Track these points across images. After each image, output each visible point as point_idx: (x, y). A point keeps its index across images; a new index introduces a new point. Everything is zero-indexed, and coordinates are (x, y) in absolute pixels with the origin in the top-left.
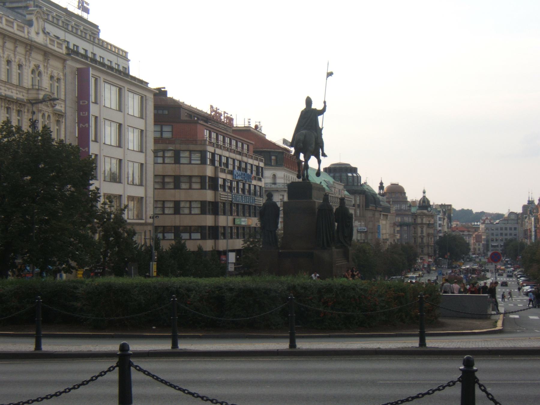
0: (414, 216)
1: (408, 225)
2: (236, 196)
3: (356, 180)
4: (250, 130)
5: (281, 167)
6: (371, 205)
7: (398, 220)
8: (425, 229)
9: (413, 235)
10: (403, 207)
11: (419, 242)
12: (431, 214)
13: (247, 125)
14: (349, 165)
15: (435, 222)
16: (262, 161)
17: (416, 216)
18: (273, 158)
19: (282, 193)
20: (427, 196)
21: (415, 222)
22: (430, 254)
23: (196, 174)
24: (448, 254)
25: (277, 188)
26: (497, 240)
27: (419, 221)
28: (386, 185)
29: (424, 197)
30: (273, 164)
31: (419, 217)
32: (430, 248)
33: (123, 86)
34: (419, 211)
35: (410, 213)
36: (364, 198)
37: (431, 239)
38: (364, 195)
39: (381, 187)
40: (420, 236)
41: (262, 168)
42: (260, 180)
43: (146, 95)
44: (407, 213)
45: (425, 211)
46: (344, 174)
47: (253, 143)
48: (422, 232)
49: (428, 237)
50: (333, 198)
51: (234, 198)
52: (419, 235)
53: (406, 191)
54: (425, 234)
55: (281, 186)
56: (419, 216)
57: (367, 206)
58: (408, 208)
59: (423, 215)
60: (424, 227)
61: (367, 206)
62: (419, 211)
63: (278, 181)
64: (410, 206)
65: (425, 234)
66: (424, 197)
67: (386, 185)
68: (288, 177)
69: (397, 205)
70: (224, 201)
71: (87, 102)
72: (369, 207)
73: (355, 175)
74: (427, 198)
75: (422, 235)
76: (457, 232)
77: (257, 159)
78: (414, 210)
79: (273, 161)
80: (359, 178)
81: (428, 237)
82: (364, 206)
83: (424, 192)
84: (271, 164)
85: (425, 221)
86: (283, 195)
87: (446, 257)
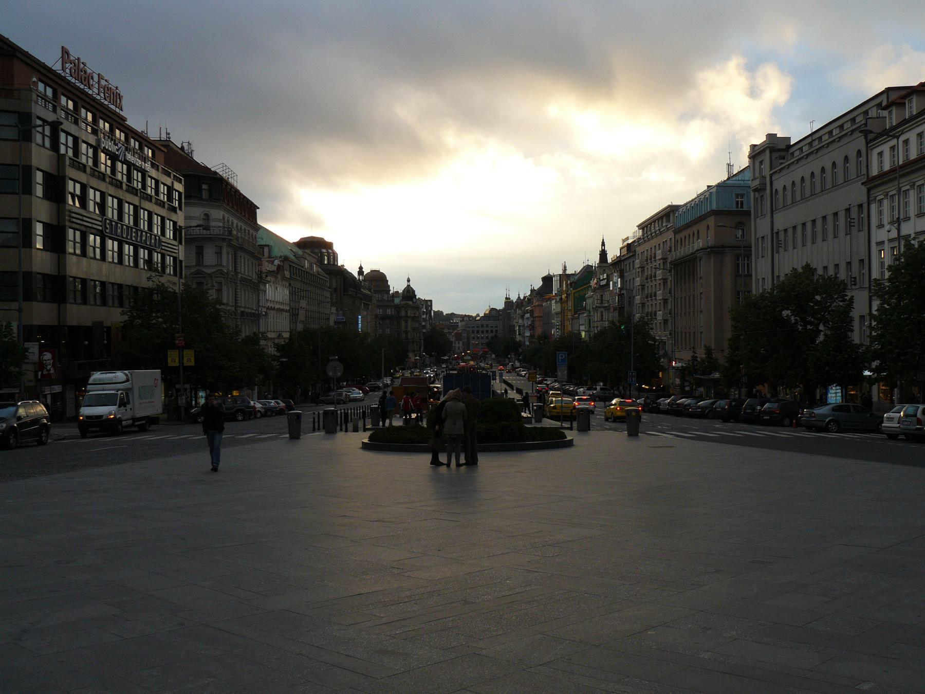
0: (398, 308)
2: (114, 223)
4: (169, 145)
6: (351, 289)
7: (380, 312)
10: (385, 297)
13: (164, 137)
15: (420, 316)
16: (180, 181)
18: (204, 187)
25: (210, 234)
26: (478, 338)
27: (403, 313)
28: (366, 271)
29: (409, 286)
30: (204, 197)
31: (403, 309)
32: (415, 344)
35: (393, 304)
37: (417, 334)
39: (361, 271)
40: (404, 331)
42: (174, 210)
45: (410, 303)
46: (317, 250)
50: (303, 272)
51: (108, 226)
55: (216, 231)
63: (213, 224)
66: (409, 286)
67: (366, 271)
68: (226, 220)
70: (83, 228)
72: (348, 292)
73: (330, 251)
77: (169, 175)
78: (397, 301)
79: (204, 192)
80: (336, 255)
83: (409, 281)
84: (201, 195)
86: (221, 247)
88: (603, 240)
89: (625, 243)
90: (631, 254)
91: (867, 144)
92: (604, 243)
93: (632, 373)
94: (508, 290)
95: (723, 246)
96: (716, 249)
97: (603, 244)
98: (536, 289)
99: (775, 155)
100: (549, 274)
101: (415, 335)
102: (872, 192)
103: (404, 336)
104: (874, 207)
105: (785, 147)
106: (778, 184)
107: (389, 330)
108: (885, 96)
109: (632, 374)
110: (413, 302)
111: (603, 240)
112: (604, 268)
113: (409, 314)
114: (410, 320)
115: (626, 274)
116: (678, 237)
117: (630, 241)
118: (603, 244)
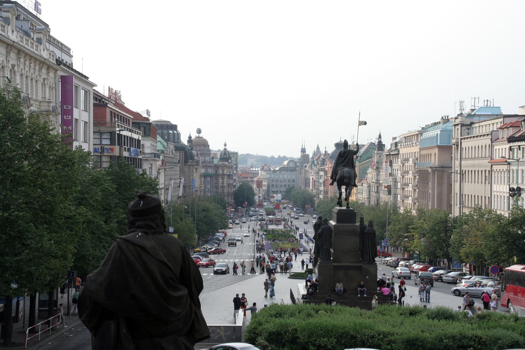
0: (217, 167)
1: (211, 176)
3: (176, 137)
5: (149, 137)
8: (225, 180)
9: (215, 185)
10: (207, 159)
14: (169, 122)
19: (151, 162)
22: (230, 203)
23: (164, 173)
24: (246, 203)
27: (220, 172)
29: (225, 149)
31: (221, 168)
32: (230, 197)
33: (79, 85)
34: (220, 163)
35: (213, 165)
36: (184, 153)
37: (231, 189)
38: (184, 152)
39: (190, 140)
40: (221, 187)
41: (140, 140)
43: (89, 89)
44: (211, 165)
45: (226, 163)
47: (132, 117)
48: (223, 183)
49: (229, 187)
52: (220, 185)
54: (225, 185)
56: (221, 167)
57: (186, 162)
58: (212, 160)
59: (224, 167)
61: (186, 162)
62: (220, 163)
64: (213, 158)
65: (225, 185)
66: (225, 149)
71: (70, 107)
72: (188, 163)
73: (175, 132)
74: (227, 151)
78: (216, 161)
80: (179, 135)
81: (229, 187)
82: (184, 161)
83: (225, 145)
85: (226, 172)
87: (244, 206)
88: (380, 134)
89: (395, 141)
90: (397, 153)
91: (492, 142)
92: (381, 136)
93: (387, 240)
94: (303, 142)
95: (442, 167)
96: (438, 169)
97: (380, 137)
98: (329, 153)
99: (464, 128)
100: (341, 141)
102: (493, 166)
103: (220, 189)
104: (493, 173)
105: (469, 123)
106: (464, 145)
107: (209, 186)
108: (501, 120)
109: (387, 241)
111: (380, 134)
112: (380, 155)
113: (225, 172)
114: (226, 178)
115: (393, 165)
116: (423, 152)
117: (397, 140)
118: (380, 137)
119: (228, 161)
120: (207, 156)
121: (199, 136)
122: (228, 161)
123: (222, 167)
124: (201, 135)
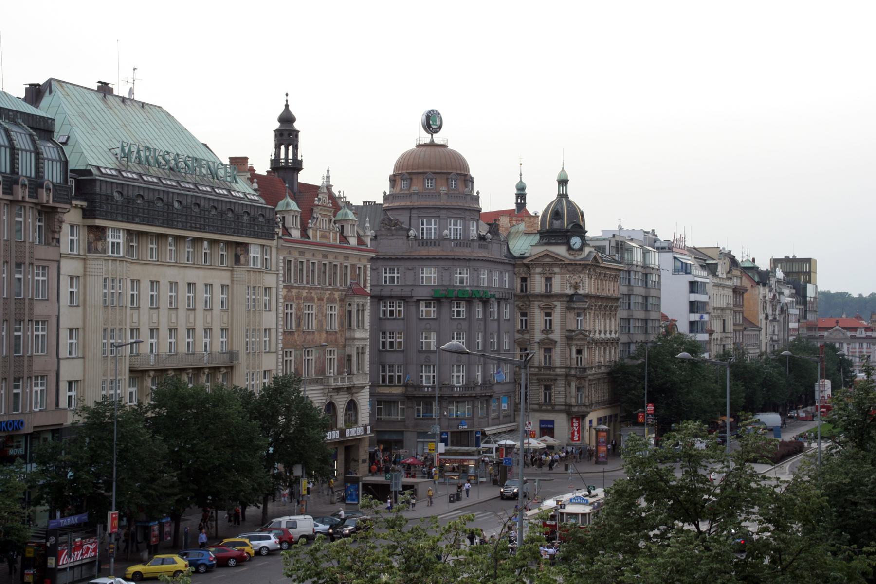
8: (556, 317)
9: (518, 336)
11: (536, 364)
12: (582, 260)
17: (527, 266)
20: (575, 195)
21: (524, 289)
22: (575, 409)
24: (650, 408)
27: (538, 285)
29: (563, 196)
31: (538, 270)
32: (573, 384)
34: (541, 249)
40: (541, 343)
45: (561, 250)
48: (548, 328)
52: (538, 336)
53: (472, 173)
54: (557, 335)
56: (538, 265)
59: (551, 265)
60: (555, 306)
65: (556, 336)
66: (563, 196)
69: (429, 224)
74: (569, 203)
75: (548, 339)
76: (837, 330)
83: (563, 182)
101: (574, 355)
110: (570, 248)
113: (556, 288)
119: (568, 244)
120: (456, 218)
121: (432, 141)
122: (568, 244)
123: (543, 265)
124: (438, 138)
